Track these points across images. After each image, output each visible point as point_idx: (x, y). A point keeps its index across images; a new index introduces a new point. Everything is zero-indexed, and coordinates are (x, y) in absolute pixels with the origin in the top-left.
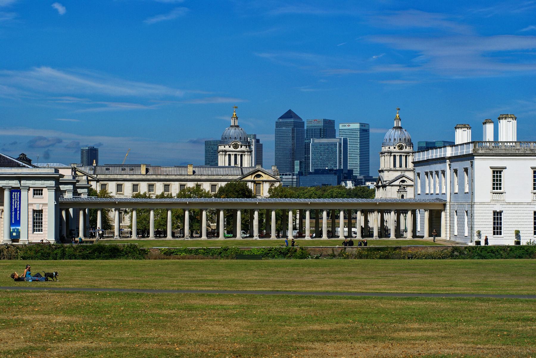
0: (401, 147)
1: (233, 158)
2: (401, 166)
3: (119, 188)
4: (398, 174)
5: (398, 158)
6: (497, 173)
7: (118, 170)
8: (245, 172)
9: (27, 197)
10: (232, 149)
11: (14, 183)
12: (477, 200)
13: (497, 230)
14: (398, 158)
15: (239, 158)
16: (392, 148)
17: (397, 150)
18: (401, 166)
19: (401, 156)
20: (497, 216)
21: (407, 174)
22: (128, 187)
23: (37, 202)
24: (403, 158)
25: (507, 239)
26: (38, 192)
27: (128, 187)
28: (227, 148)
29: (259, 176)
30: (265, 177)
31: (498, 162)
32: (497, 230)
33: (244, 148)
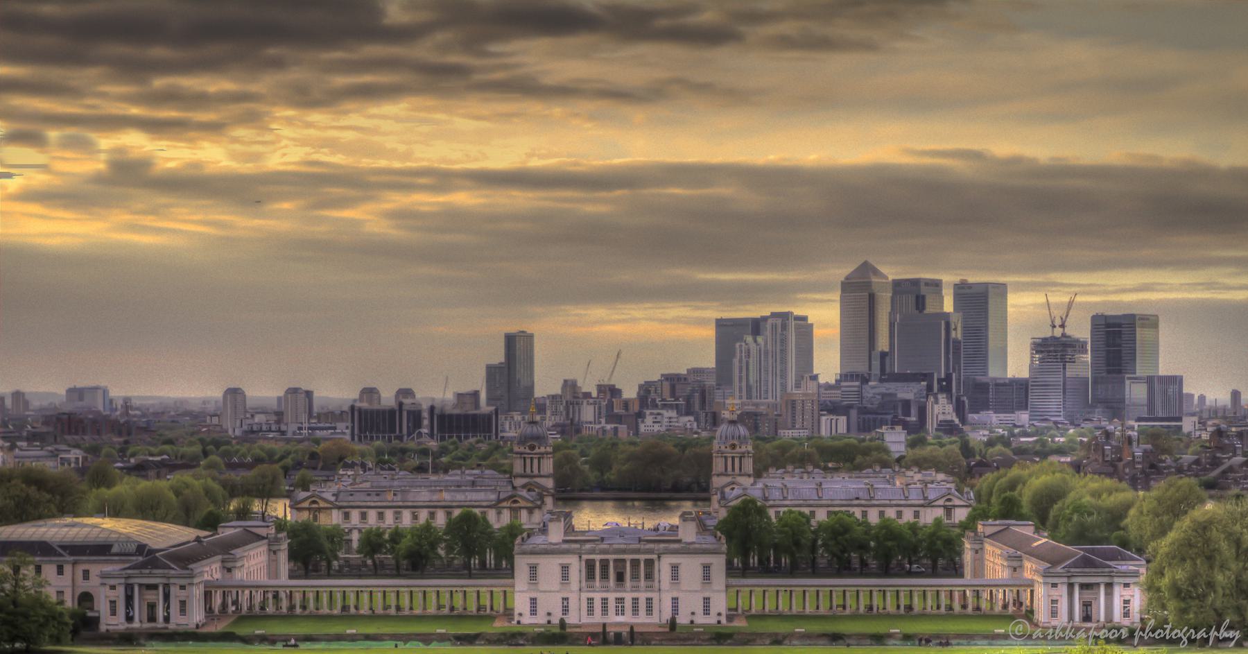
0: (733, 446)
1: (528, 461)
2: (733, 469)
3: (364, 516)
4: (729, 479)
5: (730, 461)
6: (533, 569)
7: (362, 497)
8: (502, 497)
9: (174, 591)
10: (527, 451)
11: (165, 581)
12: (517, 589)
13: (534, 612)
14: (730, 461)
15: (536, 461)
16: (723, 448)
17: (729, 450)
18: (733, 469)
19: (733, 458)
20: (534, 601)
21: (741, 480)
22: (372, 515)
23: (183, 594)
24: (737, 460)
25: (541, 619)
26: (183, 587)
27: (372, 515)
28: (522, 449)
29: (515, 502)
30: (522, 503)
31: (533, 560)
32: (534, 612)
33: (542, 450)
